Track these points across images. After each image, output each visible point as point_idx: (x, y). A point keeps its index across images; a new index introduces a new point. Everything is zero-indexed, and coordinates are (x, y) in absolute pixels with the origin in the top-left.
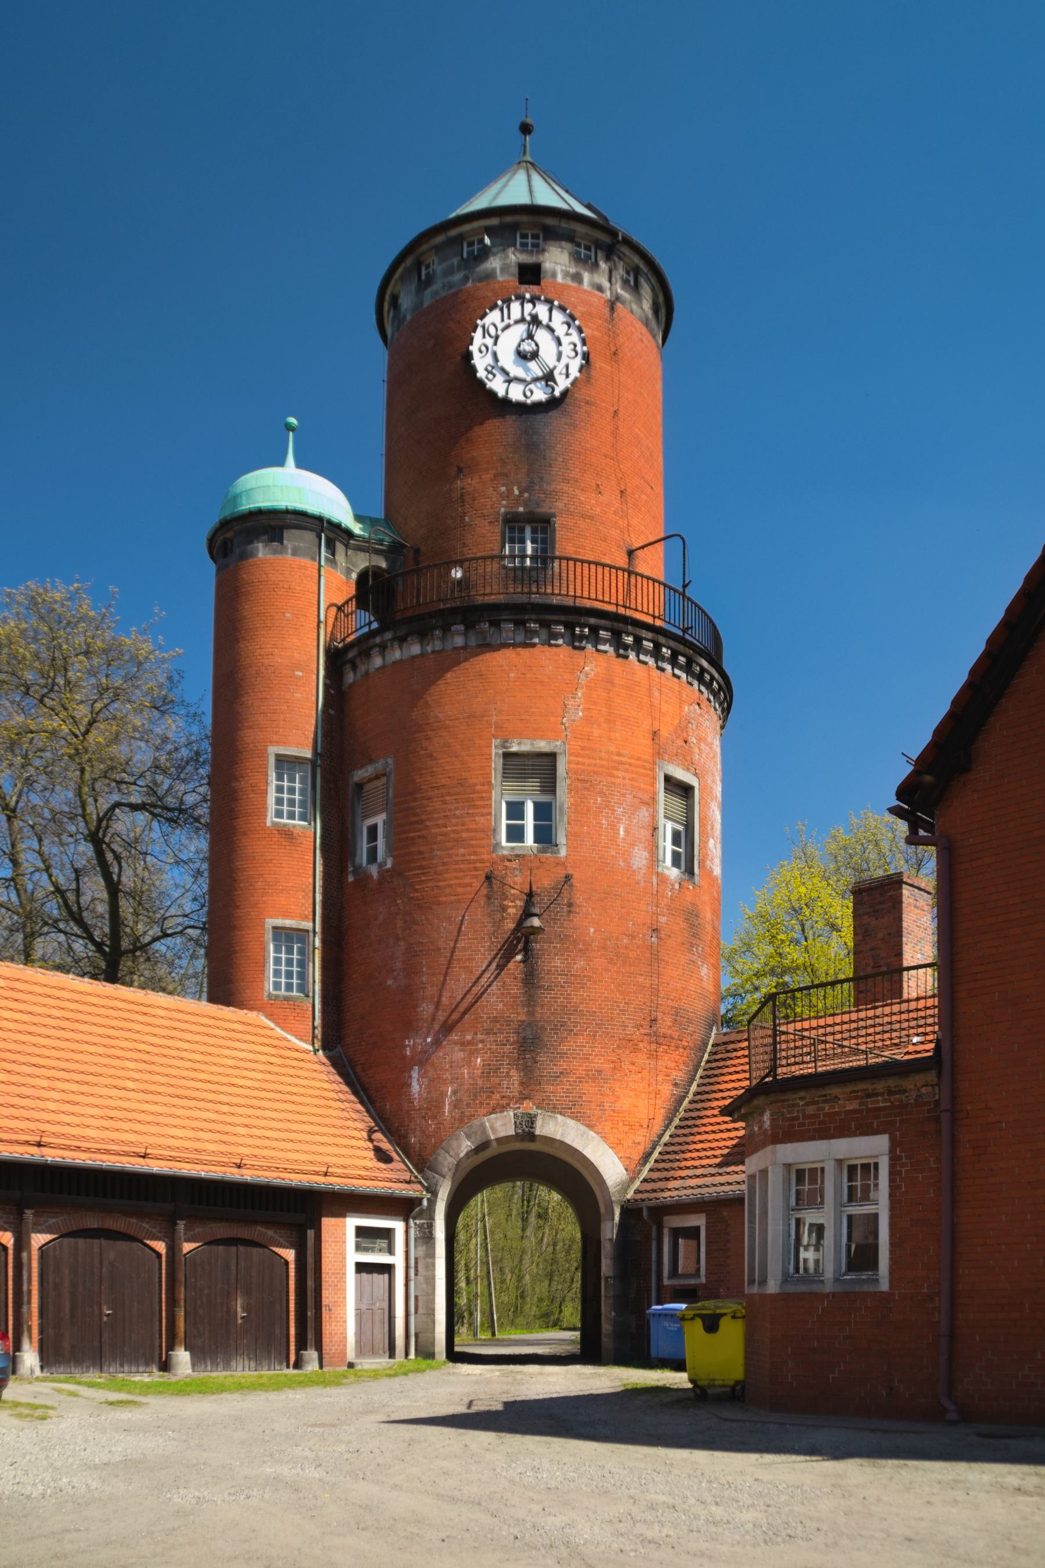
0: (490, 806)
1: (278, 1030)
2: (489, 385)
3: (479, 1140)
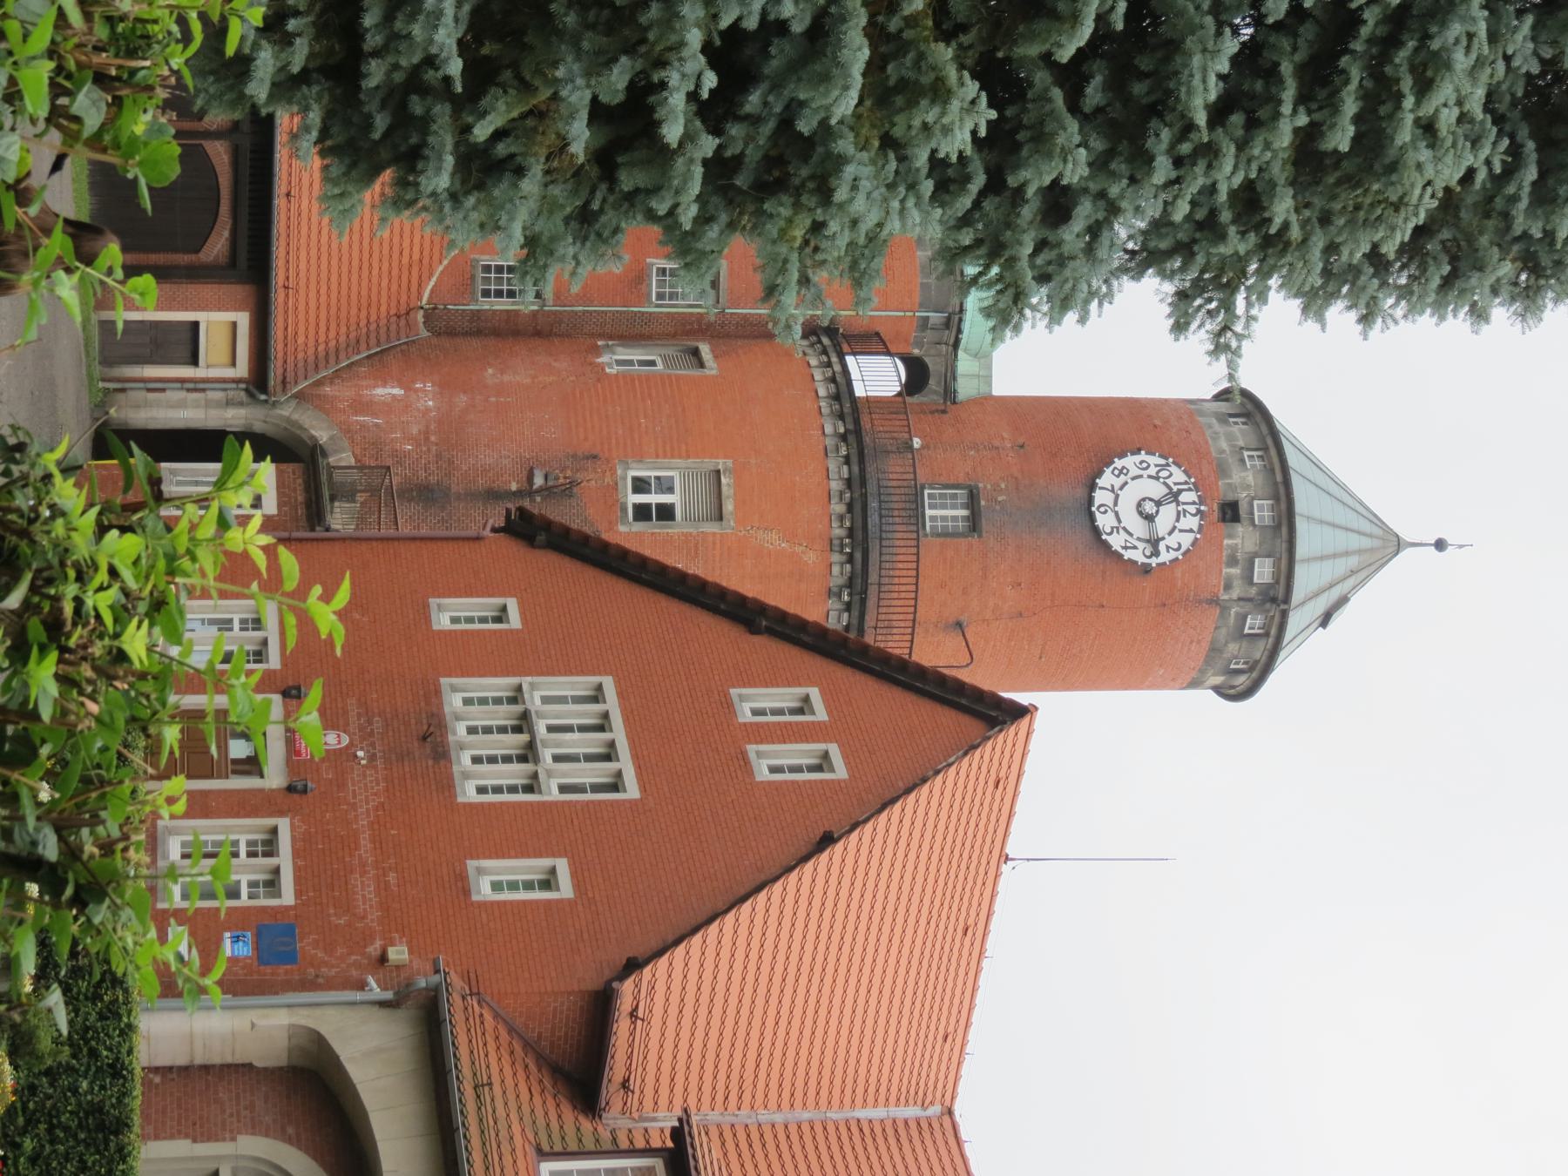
0: (665, 457)
1: (441, 268)
2: (1108, 471)
3: (328, 448)
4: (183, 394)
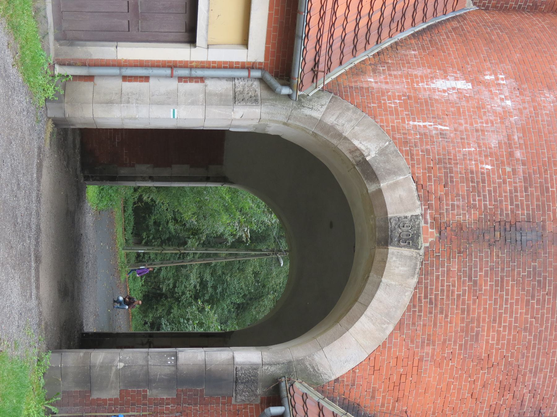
3: (378, 167)
4: (173, 84)
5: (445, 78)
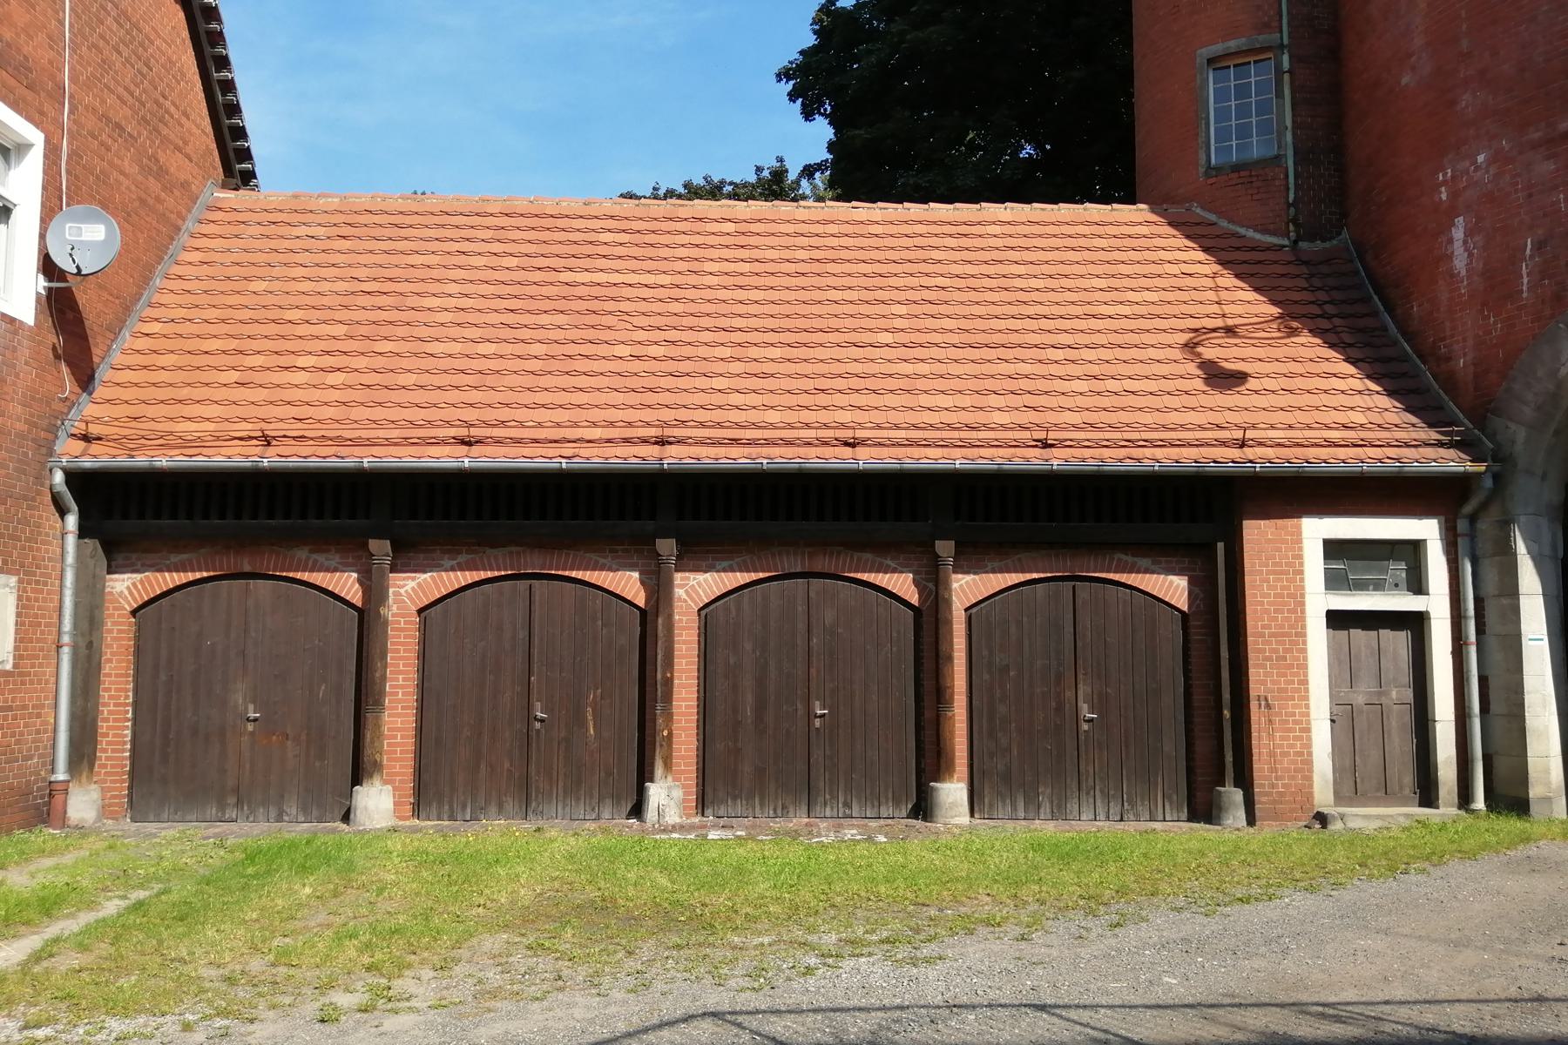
1: (1224, 224)
5: (1450, 257)
